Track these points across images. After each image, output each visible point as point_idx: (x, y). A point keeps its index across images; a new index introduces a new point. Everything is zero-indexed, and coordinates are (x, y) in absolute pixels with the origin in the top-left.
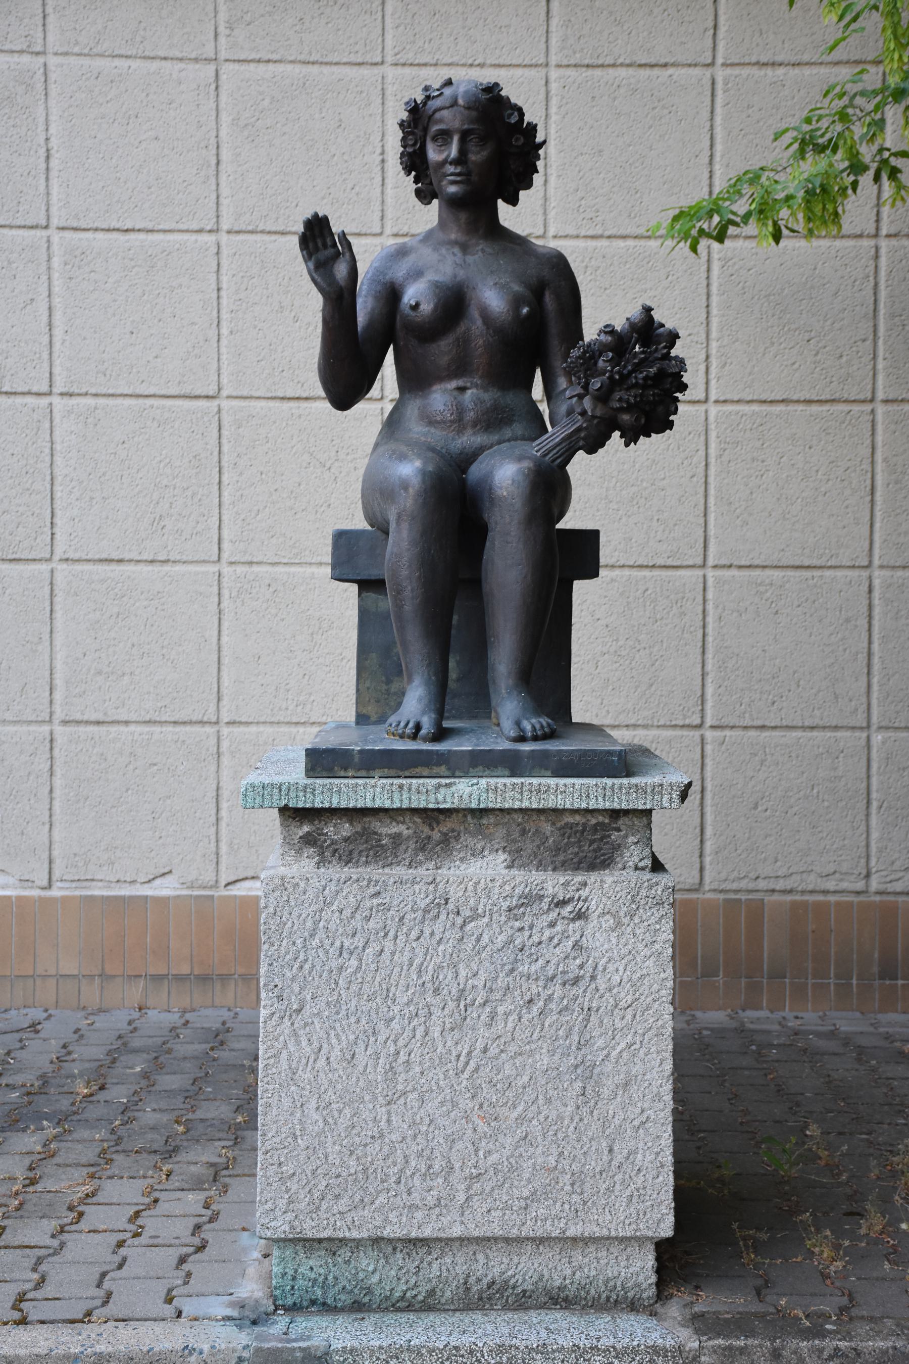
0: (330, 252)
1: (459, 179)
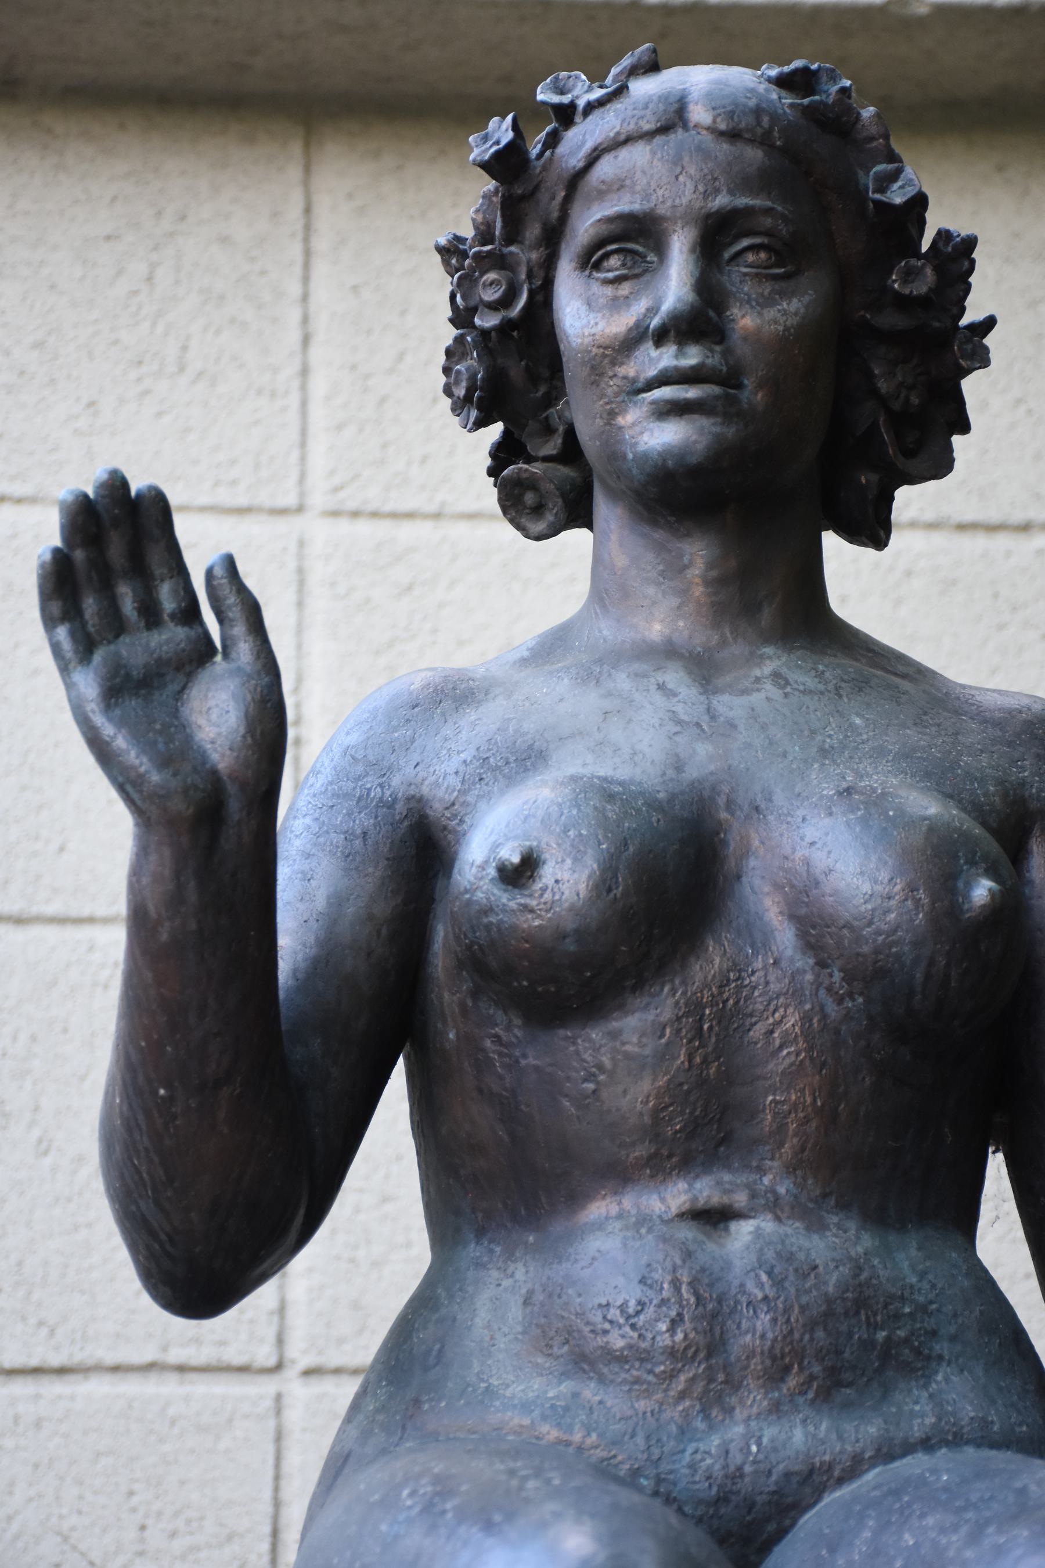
0: (171, 637)
1: (692, 393)
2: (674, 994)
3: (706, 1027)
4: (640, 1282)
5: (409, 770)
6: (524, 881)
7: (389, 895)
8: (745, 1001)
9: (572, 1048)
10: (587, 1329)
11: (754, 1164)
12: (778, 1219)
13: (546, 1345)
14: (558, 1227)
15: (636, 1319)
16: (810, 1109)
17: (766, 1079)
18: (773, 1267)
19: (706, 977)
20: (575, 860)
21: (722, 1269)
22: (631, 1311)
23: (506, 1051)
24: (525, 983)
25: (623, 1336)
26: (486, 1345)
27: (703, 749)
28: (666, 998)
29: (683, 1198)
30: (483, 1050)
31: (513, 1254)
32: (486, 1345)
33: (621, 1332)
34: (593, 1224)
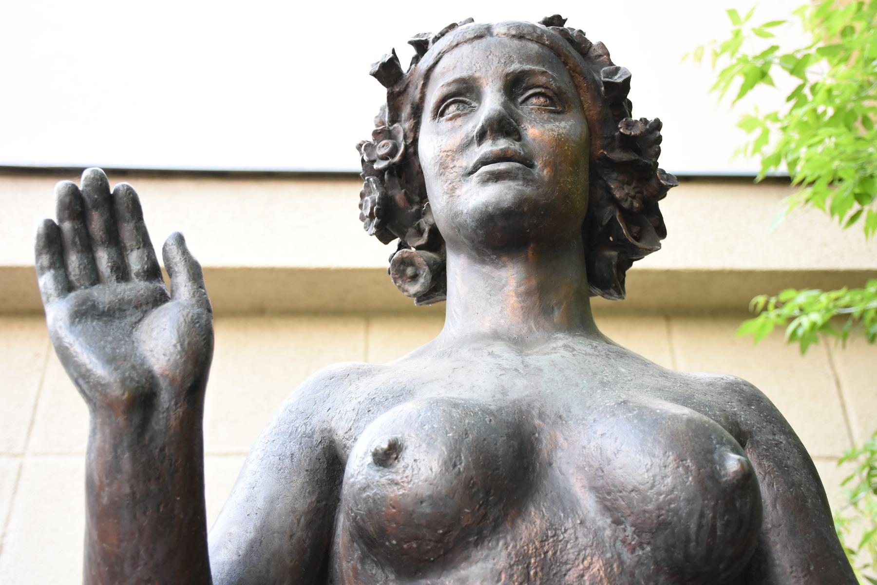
0: (138, 287)
1: (502, 166)
3: (532, 573)
6: (391, 461)
8: (561, 552)
19: (530, 534)
20: (429, 444)
24: (394, 542)
27: (520, 383)
28: (501, 551)
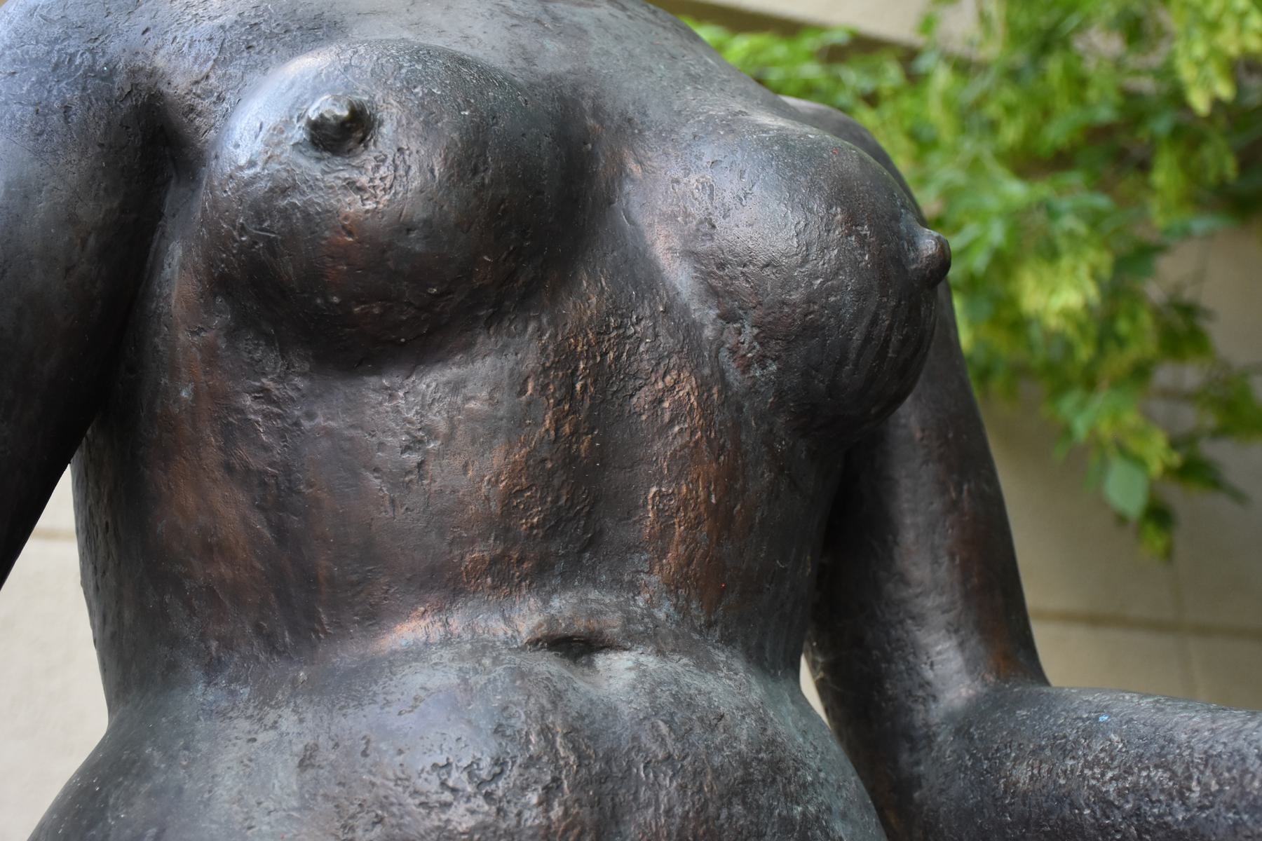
2: (541, 336)
3: (578, 386)
4: (496, 731)
5: (135, 36)
6: (351, 144)
7: (102, 193)
8: (629, 357)
9: (387, 405)
10: (412, 803)
11: (626, 578)
12: (660, 652)
13: (344, 827)
14: (346, 655)
15: (493, 786)
16: (702, 508)
17: (651, 463)
18: (672, 715)
19: (581, 319)
20: (426, 123)
21: (606, 716)
22: (484, 774)
23: (276, 410)
24: (336, 300)
25: (473, 812)
26: (237, 827)
27: (553, 46)
28: (530, 340)
29: (537, 619)
30: (241, 411)
31: (272, 697)
32: (237, 827)
33: (468, 805)
34: (406, 653)
